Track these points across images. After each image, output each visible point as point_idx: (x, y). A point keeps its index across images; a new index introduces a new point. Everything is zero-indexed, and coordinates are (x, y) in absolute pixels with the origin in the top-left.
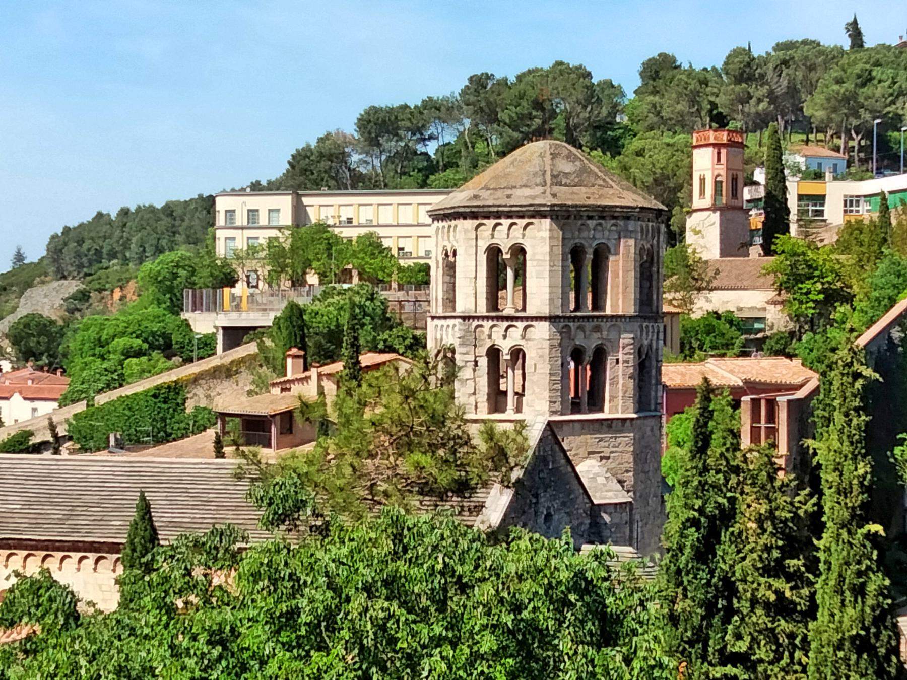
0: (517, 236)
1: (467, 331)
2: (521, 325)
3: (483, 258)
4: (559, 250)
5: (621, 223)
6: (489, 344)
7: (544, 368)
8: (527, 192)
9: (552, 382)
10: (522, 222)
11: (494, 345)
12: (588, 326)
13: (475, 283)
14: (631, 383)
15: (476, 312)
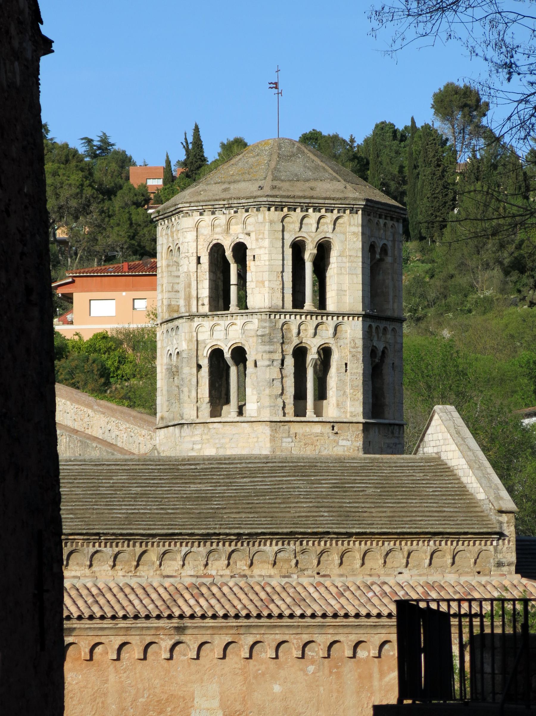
1: (273, 328)
2: (331, 322)
3: (289, 252)
5: (396, 224)
6: (295, 341)
10: (330, 217)
11: (301, 343)
13: (282, 277)
15: (283, 308)
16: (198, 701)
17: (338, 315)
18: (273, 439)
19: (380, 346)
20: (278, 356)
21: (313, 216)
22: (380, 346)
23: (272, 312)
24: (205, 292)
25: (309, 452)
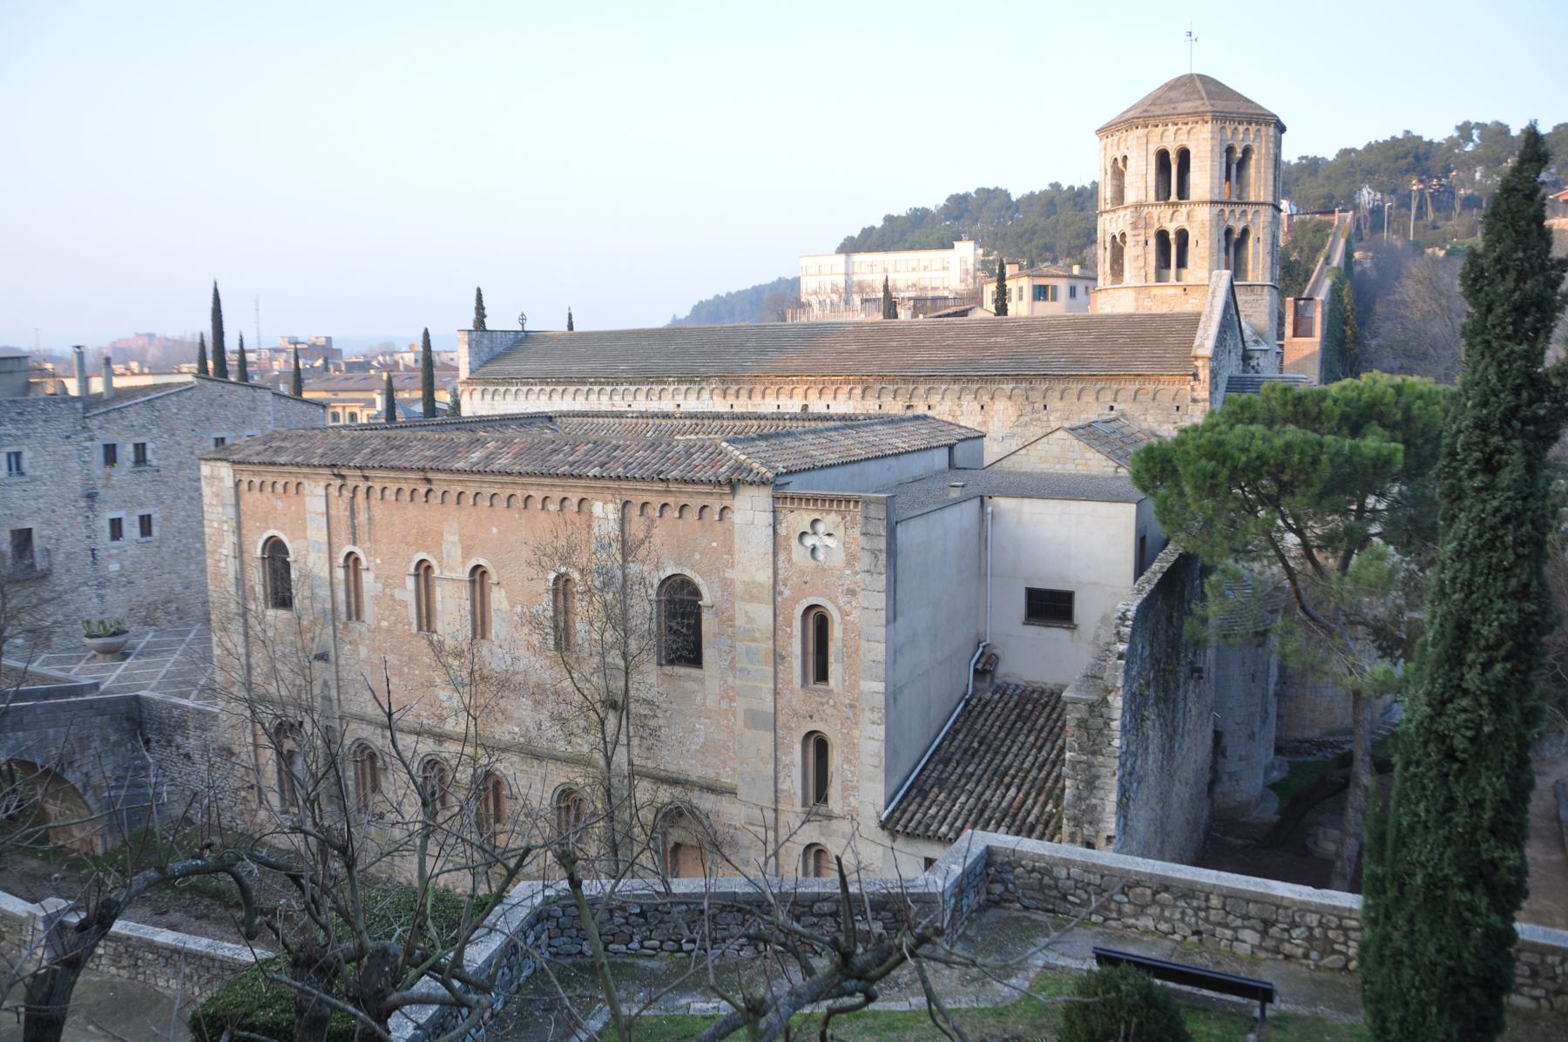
0: (1183, 140)
4: (1217, 149)
6: (1157, 226)
7: (1205, 244)
8: (1190, 104)
9: (1211, 254)
12: (1238, 210)
14: (1268, 259)
16: (446, 535)
17: (1256, 204)
18: (1137, 300)
19: (1238, 227)
20: (1142, 238)
21: (1172, 128)
22: (1238, 227)
23: (1138, 206)
24: (1109, 195)
25: (1164, 310)
